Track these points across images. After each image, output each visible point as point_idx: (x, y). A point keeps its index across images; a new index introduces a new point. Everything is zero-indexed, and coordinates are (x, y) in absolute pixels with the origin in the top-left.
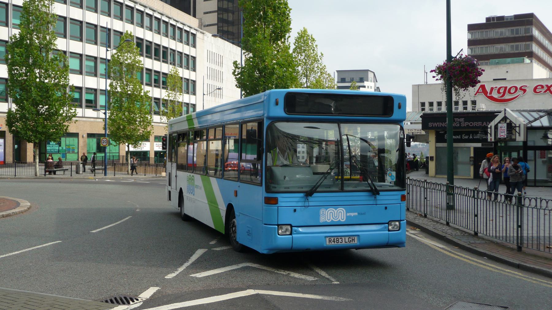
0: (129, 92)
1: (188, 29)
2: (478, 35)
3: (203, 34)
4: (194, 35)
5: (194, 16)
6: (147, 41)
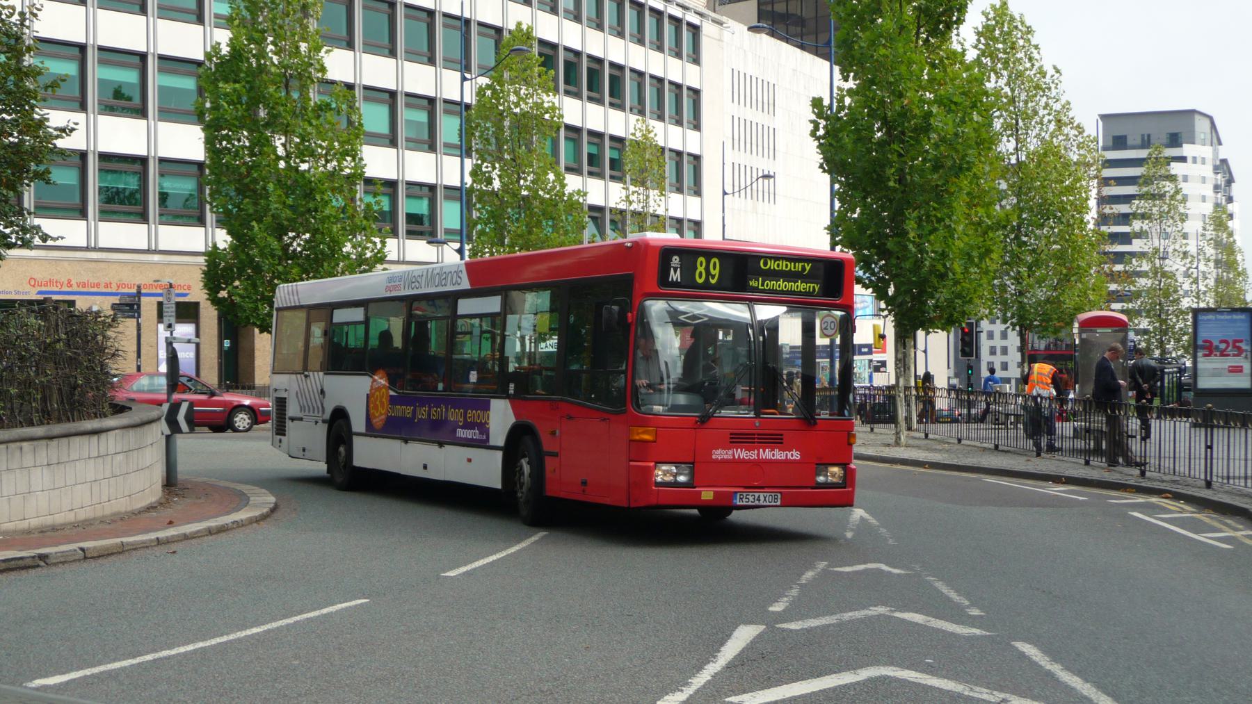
0: (525, 193)
3: (721, 24)
4: (695, 29)
6: (567, 49)
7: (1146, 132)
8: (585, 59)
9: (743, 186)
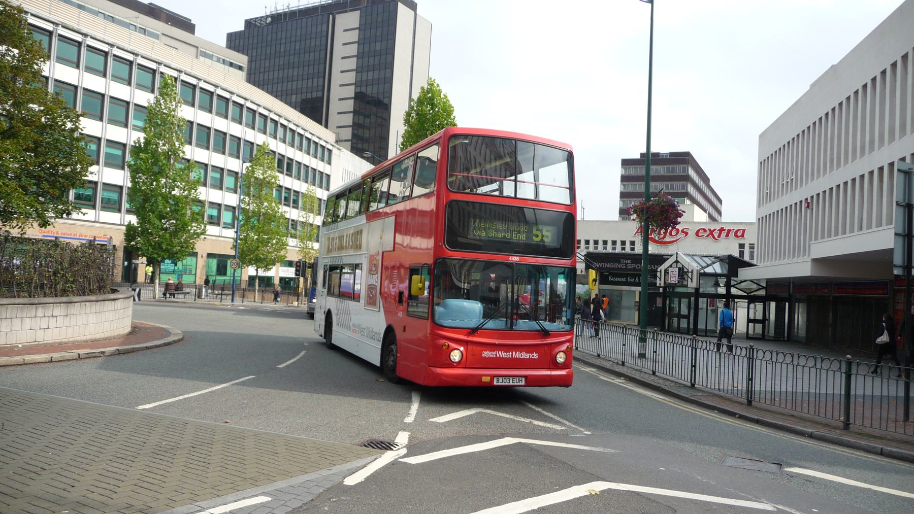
1: (324, 144)
2: (632, 171)
4: (330, 151)
5: (326, 127)
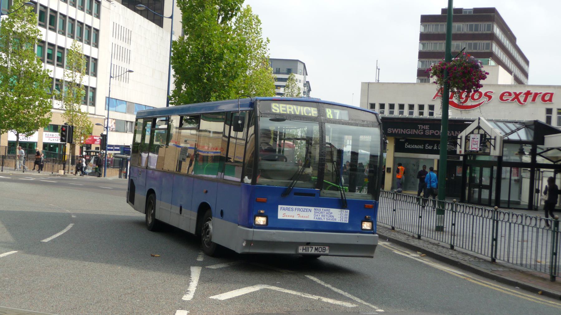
2: (432, 29)
6: (41, 5)
7: (278, 68)
8: (49, 11)
9: (117, 75)
